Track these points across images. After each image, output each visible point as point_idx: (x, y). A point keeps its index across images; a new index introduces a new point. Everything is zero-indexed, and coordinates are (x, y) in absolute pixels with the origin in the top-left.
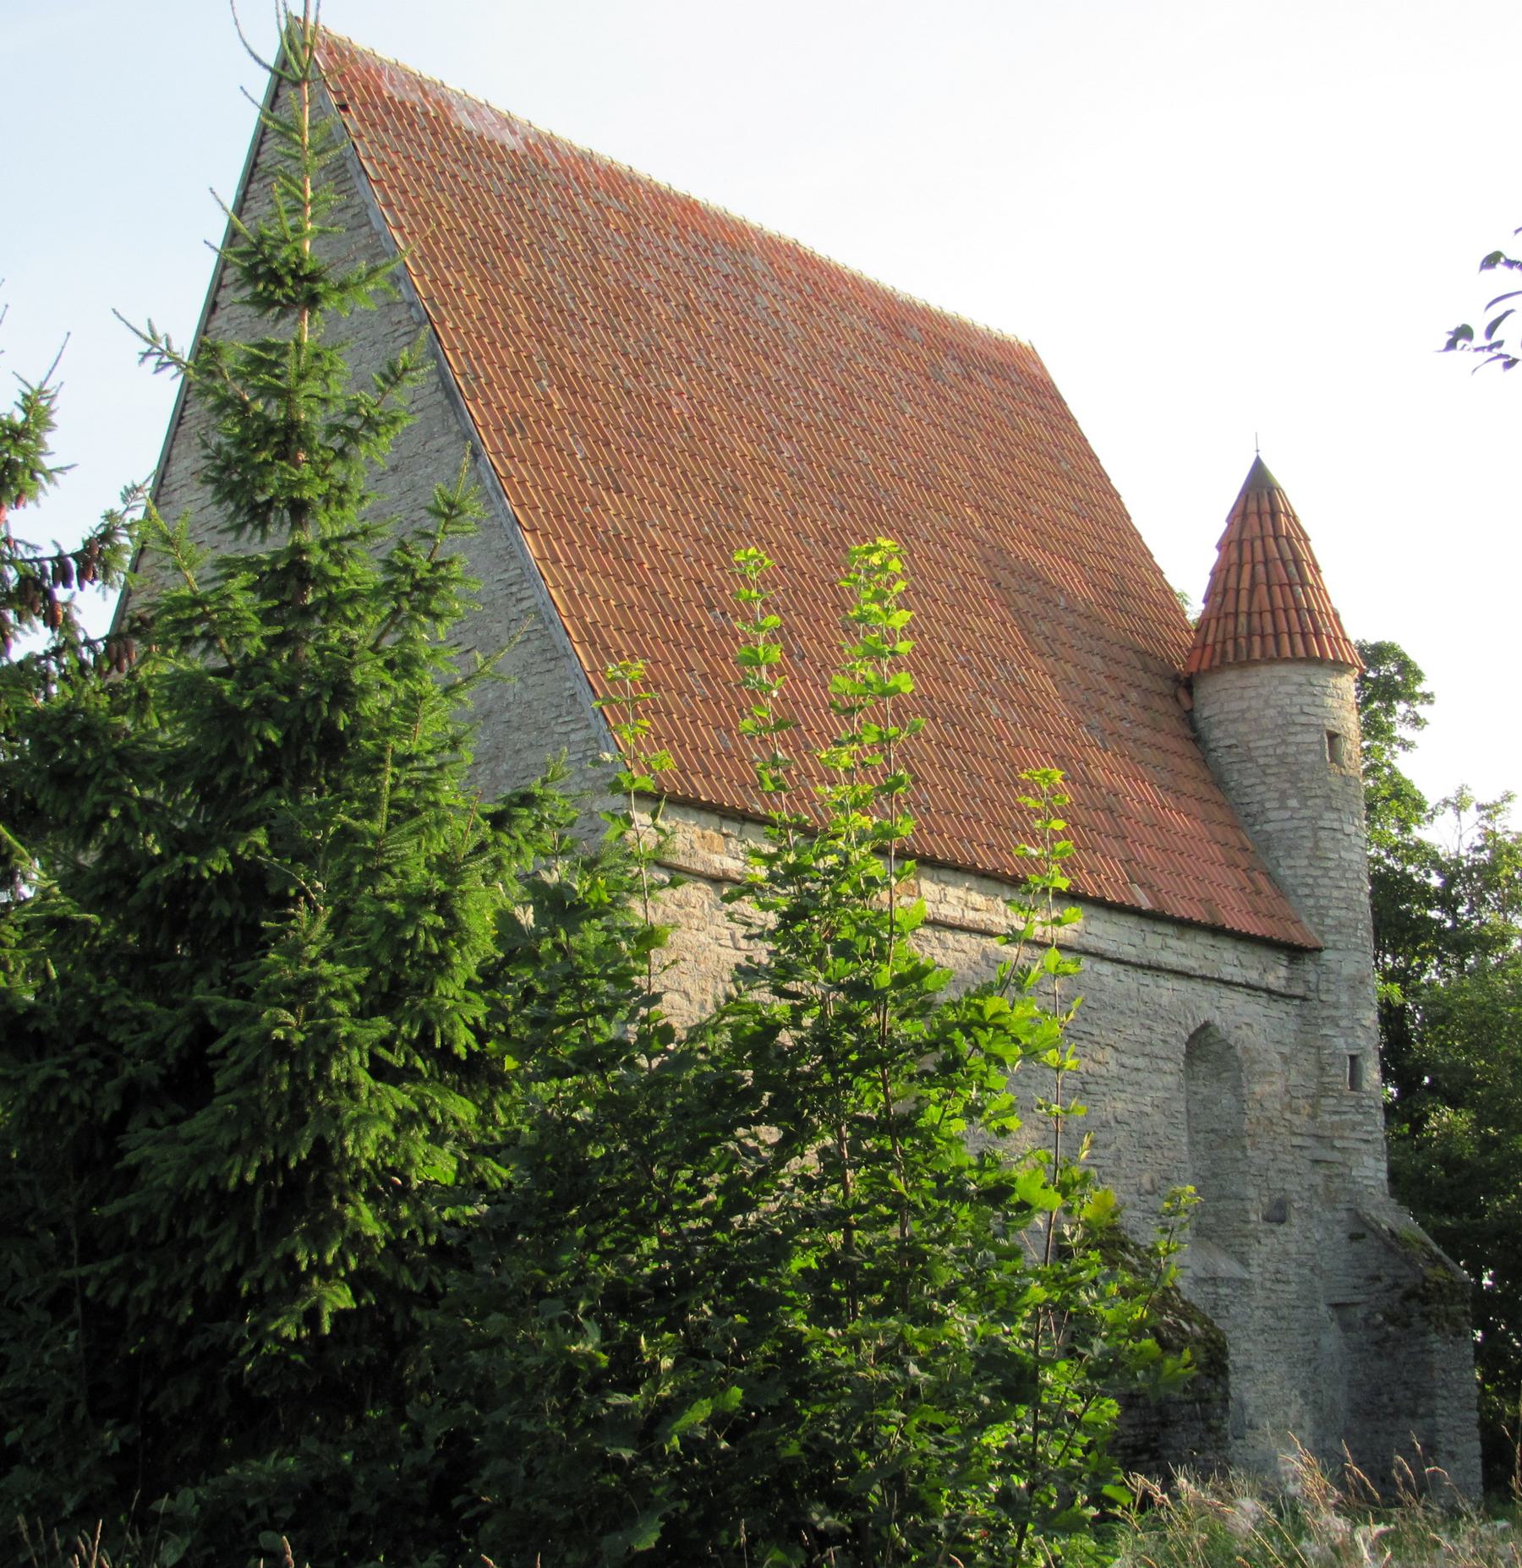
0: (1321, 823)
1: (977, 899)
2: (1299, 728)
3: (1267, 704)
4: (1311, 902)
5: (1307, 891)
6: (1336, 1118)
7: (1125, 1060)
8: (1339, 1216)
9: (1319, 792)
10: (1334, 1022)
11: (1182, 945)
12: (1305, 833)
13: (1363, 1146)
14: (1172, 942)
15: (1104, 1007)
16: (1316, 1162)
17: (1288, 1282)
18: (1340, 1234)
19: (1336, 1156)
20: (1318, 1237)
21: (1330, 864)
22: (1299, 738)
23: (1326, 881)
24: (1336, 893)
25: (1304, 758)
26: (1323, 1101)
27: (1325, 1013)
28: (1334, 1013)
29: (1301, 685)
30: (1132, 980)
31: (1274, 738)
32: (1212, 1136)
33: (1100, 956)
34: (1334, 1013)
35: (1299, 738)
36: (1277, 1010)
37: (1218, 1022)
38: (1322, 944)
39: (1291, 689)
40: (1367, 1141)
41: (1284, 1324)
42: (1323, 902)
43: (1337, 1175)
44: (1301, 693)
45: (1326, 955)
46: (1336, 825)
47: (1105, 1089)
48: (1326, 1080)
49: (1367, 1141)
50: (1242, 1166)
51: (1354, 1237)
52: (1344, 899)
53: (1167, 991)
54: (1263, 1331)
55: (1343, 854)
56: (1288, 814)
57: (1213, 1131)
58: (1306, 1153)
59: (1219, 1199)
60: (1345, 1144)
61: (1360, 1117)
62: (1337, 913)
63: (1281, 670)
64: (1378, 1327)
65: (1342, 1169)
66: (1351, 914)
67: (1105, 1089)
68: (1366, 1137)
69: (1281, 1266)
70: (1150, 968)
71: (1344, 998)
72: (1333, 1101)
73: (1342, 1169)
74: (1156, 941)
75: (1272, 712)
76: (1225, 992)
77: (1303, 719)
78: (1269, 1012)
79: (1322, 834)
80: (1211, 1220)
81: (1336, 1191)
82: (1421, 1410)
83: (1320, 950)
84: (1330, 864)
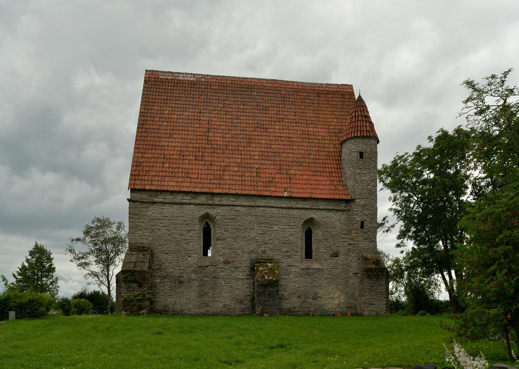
0: (356, 172)
1: (234, 200)
2: (353, 153)
3: (348, 149)
4: (353, 190)
5: (352, 187)
6: (357, 235)
7: (279, 226)
8: (356, 255)
9: (356, 166)
10: (357, 214)
11: (305, 203)
12: (353, 175)
13: (364, 240)
14: (301, 202)
15: (273, 217)
16: (350, 244)
17: (338, 269)
18: (355, 258)
19: (356, 243)
20: (350, 259)
21: (358, 181)
22: (353, 155)
23: (357, 185)
24: (359, 187)
25: (353, 159)
26: (353, 231)
27: (355, 213)
28: (357, 212)
29: (354, 143)
30: (284, 211)
31: (348, 156)
32: (317, 240)
33: (272, 207)
34: (357, 212)
35: (353, 155)
36: (338, 214)
37: (315, 216)
38: (353, 197)
39: (351, 144)
40: (366, 239)
41: (335, 277)
42: (356, 189)
43: (356, 247)
44: (354, 145)
45: (356, 201)
46: (360, 172)
47: (271, 233)
48: (354, 227)
49: (366, 239)
50: (323, 246)
51: (358, 259)
52: (362, 188)
53: (295, 212)
54: (327, 279)
55: (362, 178)
56: (350, 172)
57: (318, 239)
58: (347, 242)
59: (320, 252)
60: (359, 240)
61: (363, 234)
62: (359, 191)
63: (350, 141)
64: (361, 278)
65: (357, 245)
66: (364, 191)
67: (271, 233)
68: (365, 238)
69: (335, 266)
70: (291, 208)
71: (360, 209)
72: (355, 231)
73: (357, 245)
74: (295, 203)
75: (348, 150)
76: (300, 211)
77: (354, 150)
78: (337, 214)
79: (357, 174)
80: (317, 257)
81: (355, 250)
82: (364, 295)
83: (354, 200)
84: (358, 181)
